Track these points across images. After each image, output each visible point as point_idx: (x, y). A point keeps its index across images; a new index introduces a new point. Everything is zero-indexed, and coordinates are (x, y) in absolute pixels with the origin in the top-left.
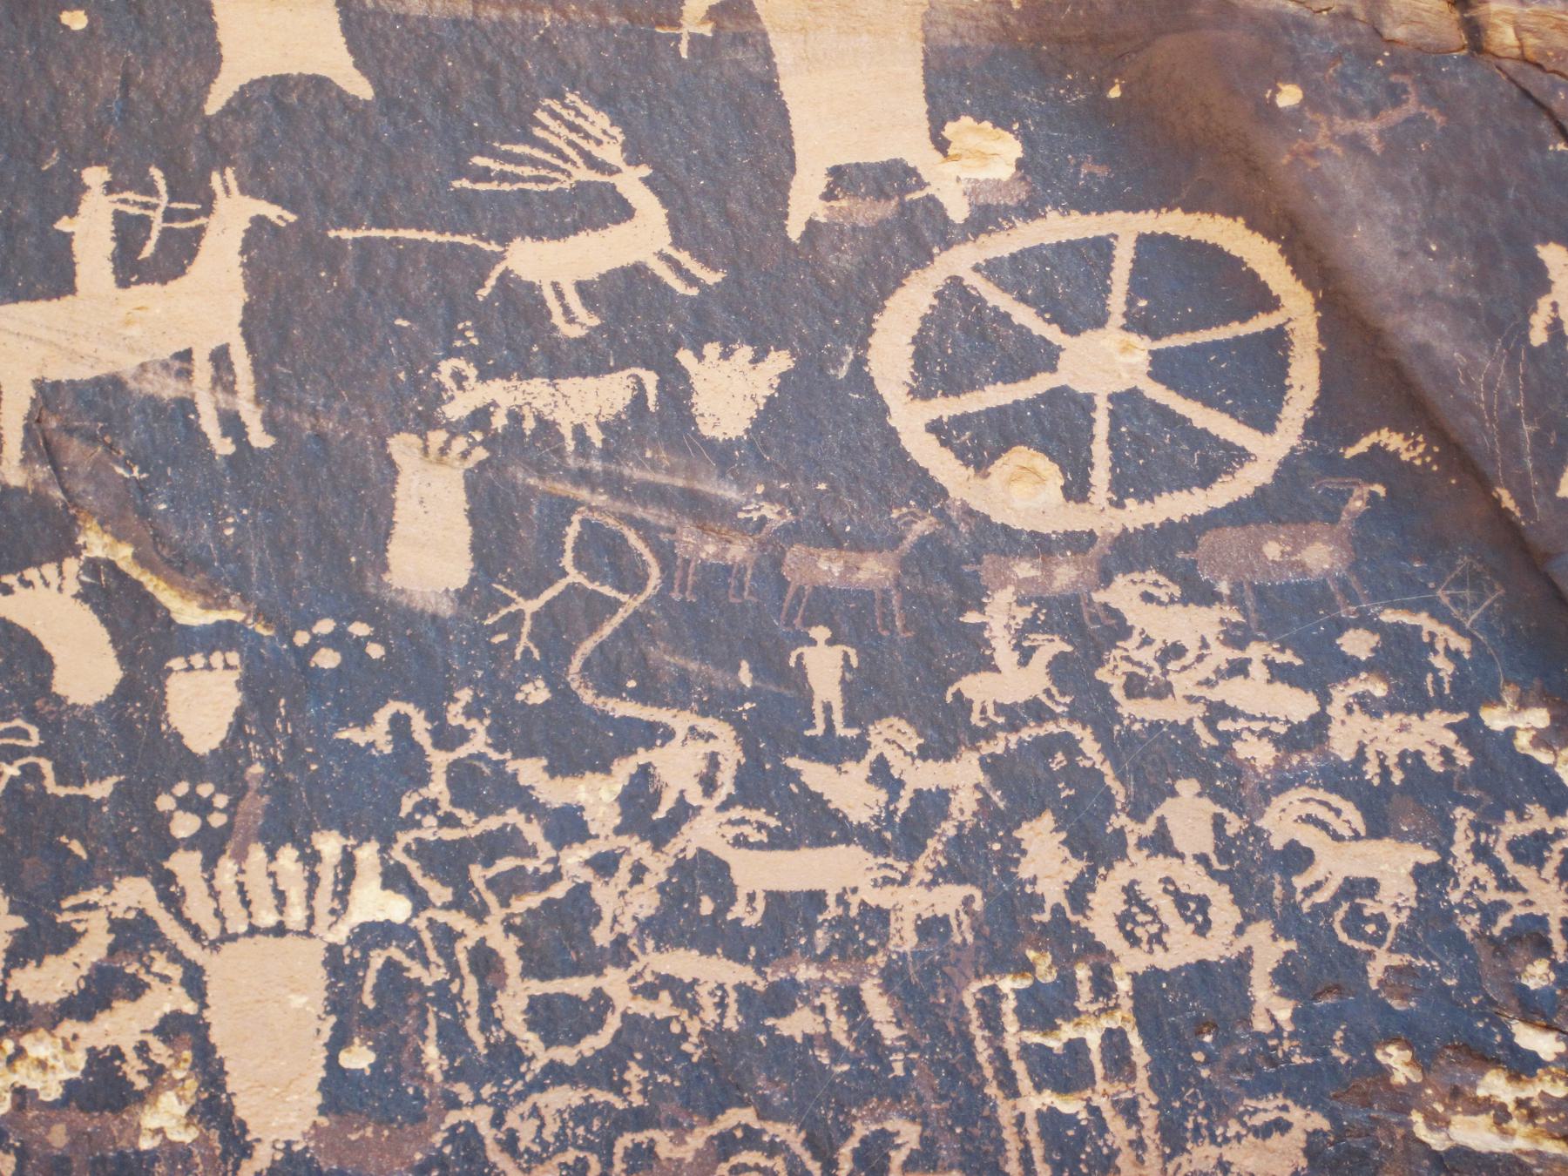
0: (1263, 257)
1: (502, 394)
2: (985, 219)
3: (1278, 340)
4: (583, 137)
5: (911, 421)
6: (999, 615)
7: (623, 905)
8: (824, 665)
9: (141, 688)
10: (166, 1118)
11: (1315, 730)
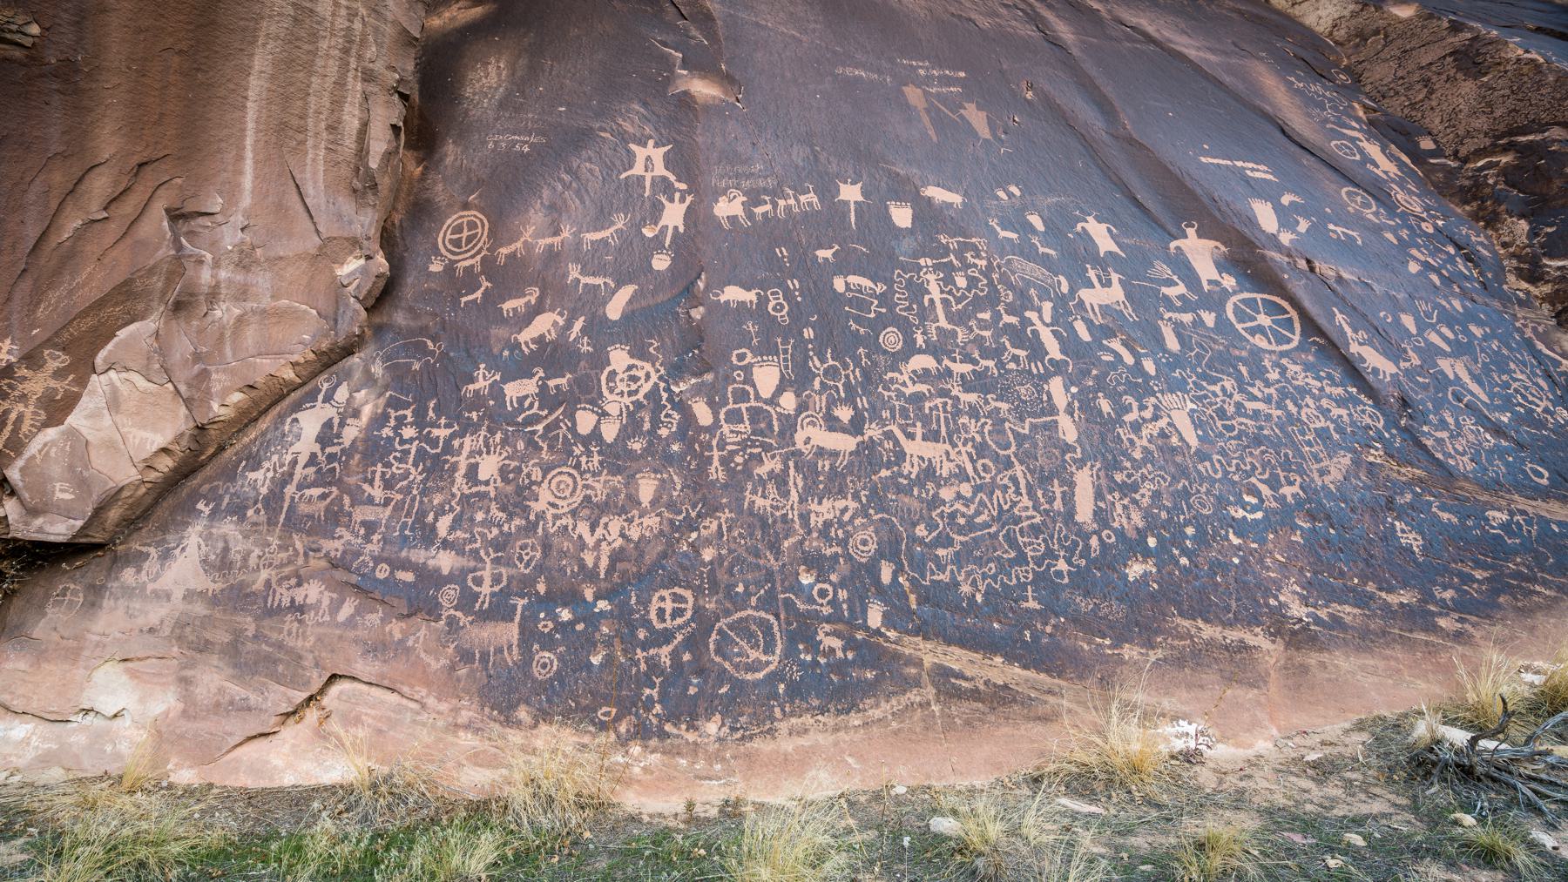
0: (1285, 304)
1: (1174, 316)
2: (1235, 293)
3: (1290, 319)
4: (1163, 270)
5: (1239, 327)
6: (1267, 363)
7: (1231, 410)
8: (1243, 369)
9: (1138, 363)
10: (1174, 440)
11: (1321, 389)
